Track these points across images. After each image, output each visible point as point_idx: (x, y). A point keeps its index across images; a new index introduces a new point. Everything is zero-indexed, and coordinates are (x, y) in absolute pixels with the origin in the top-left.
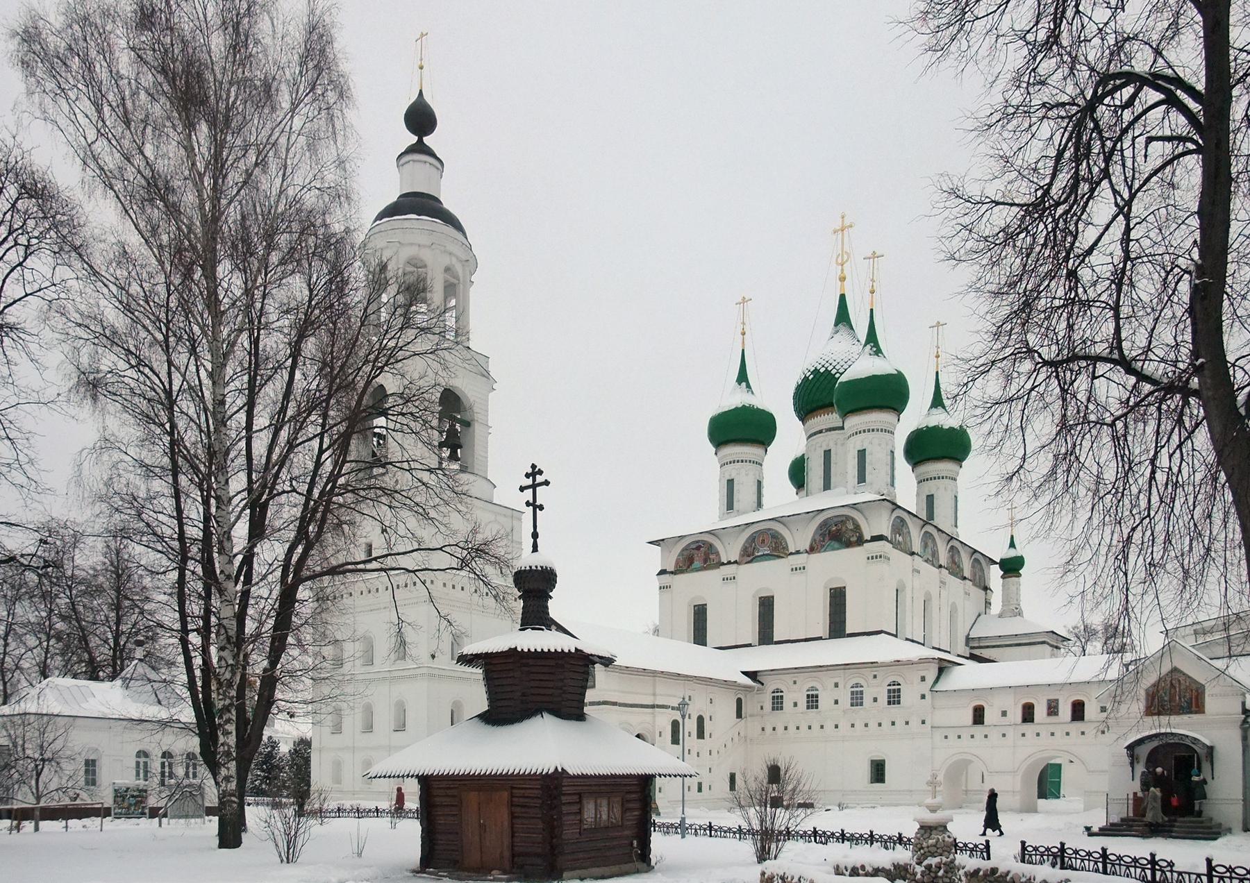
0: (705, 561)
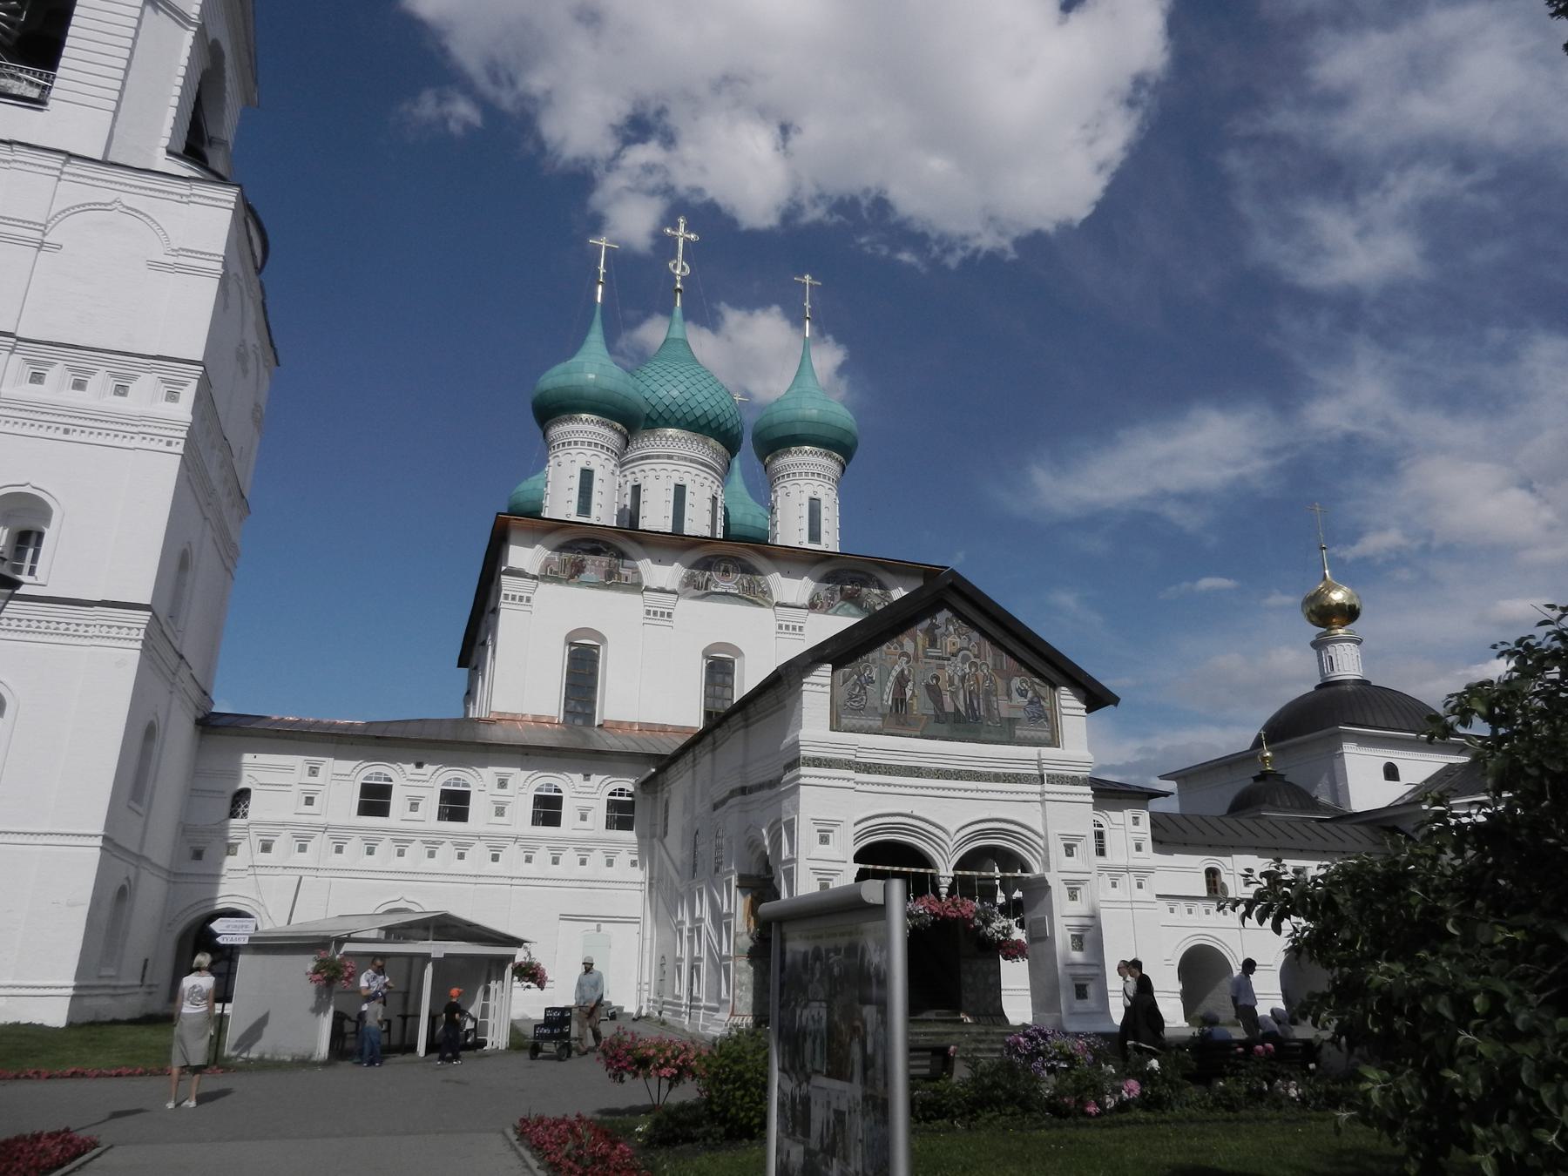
0: (610, 575)
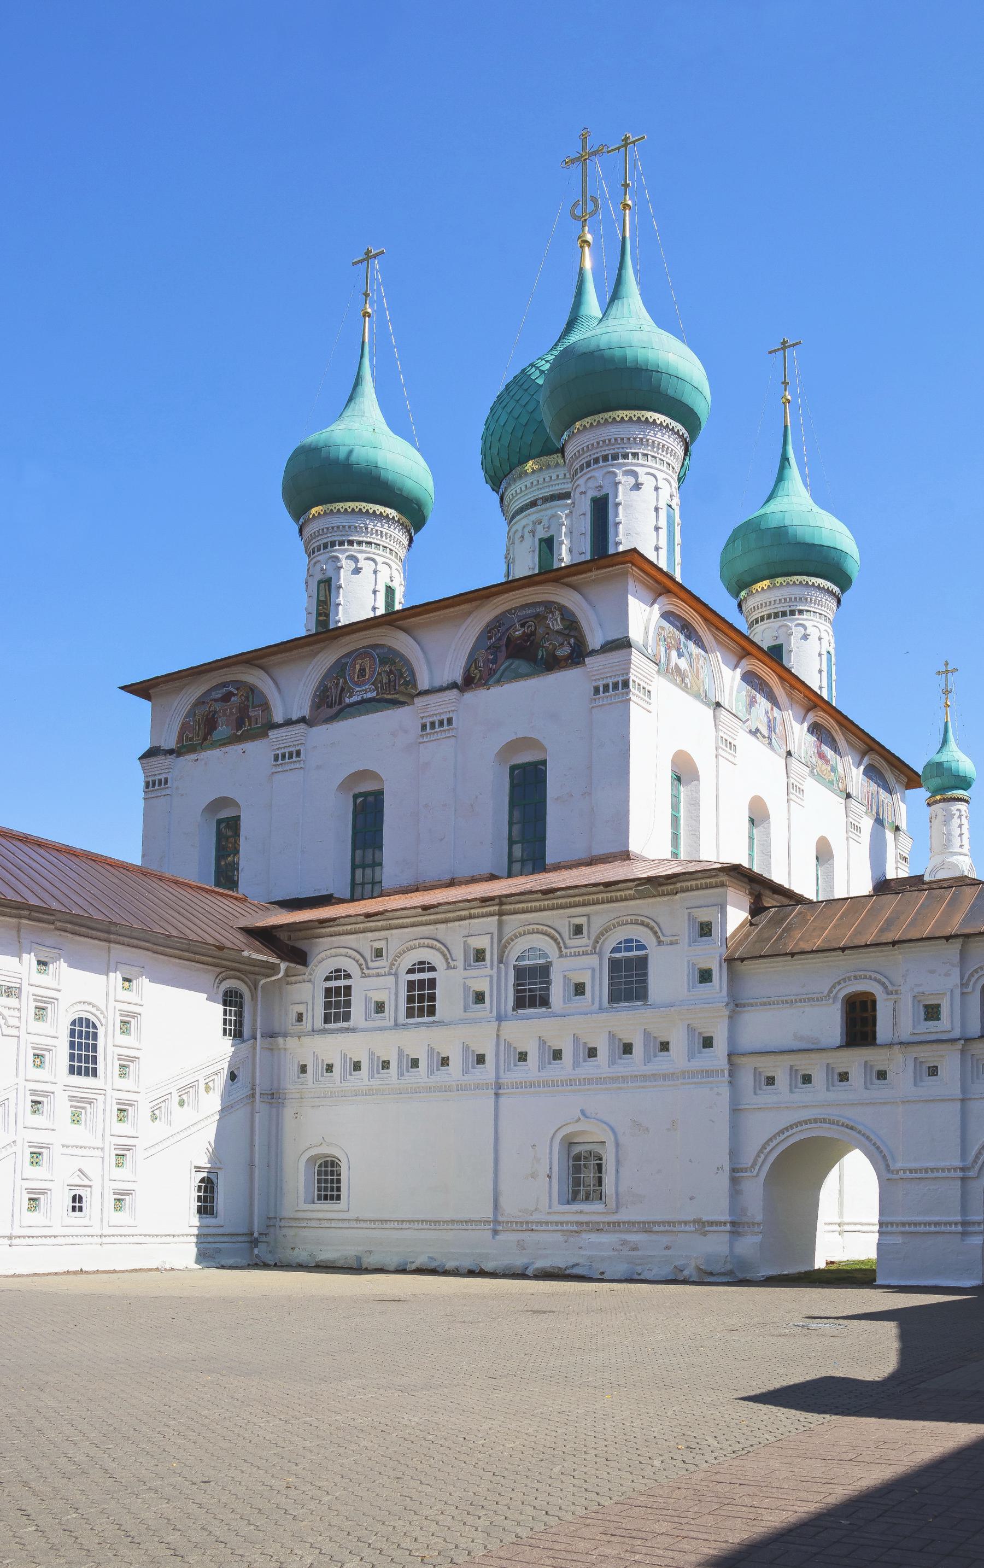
0: (239, 724)
